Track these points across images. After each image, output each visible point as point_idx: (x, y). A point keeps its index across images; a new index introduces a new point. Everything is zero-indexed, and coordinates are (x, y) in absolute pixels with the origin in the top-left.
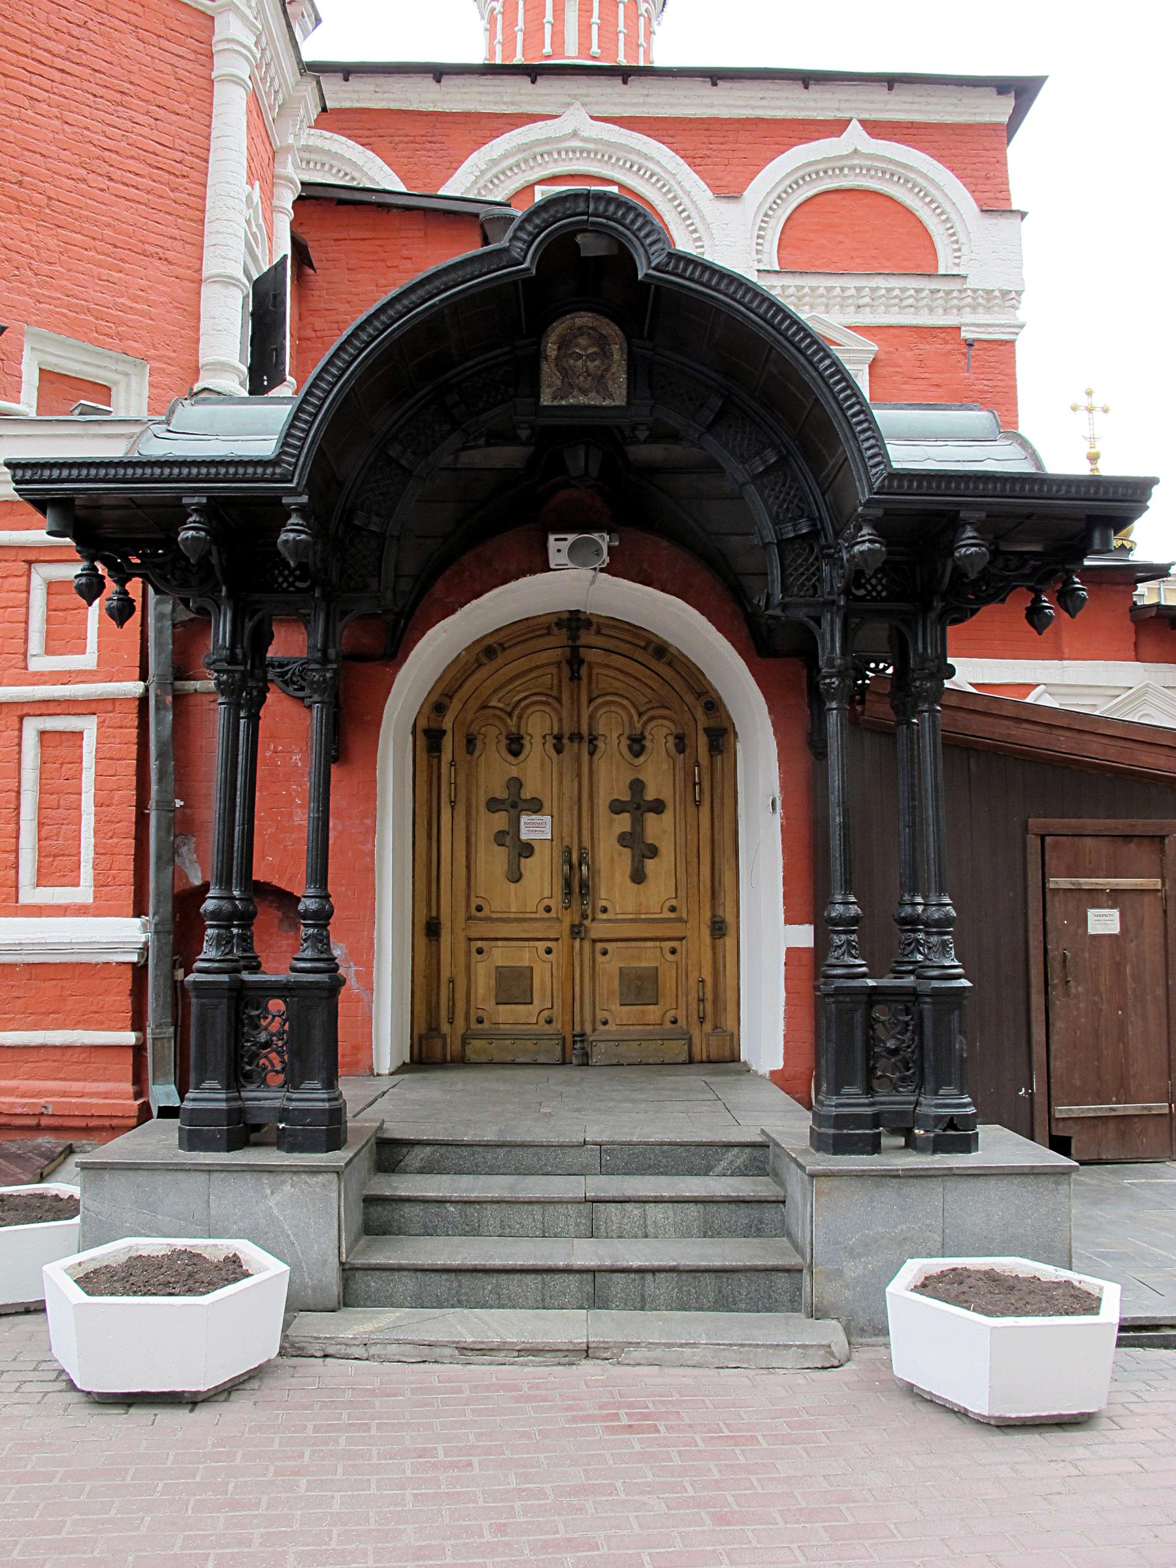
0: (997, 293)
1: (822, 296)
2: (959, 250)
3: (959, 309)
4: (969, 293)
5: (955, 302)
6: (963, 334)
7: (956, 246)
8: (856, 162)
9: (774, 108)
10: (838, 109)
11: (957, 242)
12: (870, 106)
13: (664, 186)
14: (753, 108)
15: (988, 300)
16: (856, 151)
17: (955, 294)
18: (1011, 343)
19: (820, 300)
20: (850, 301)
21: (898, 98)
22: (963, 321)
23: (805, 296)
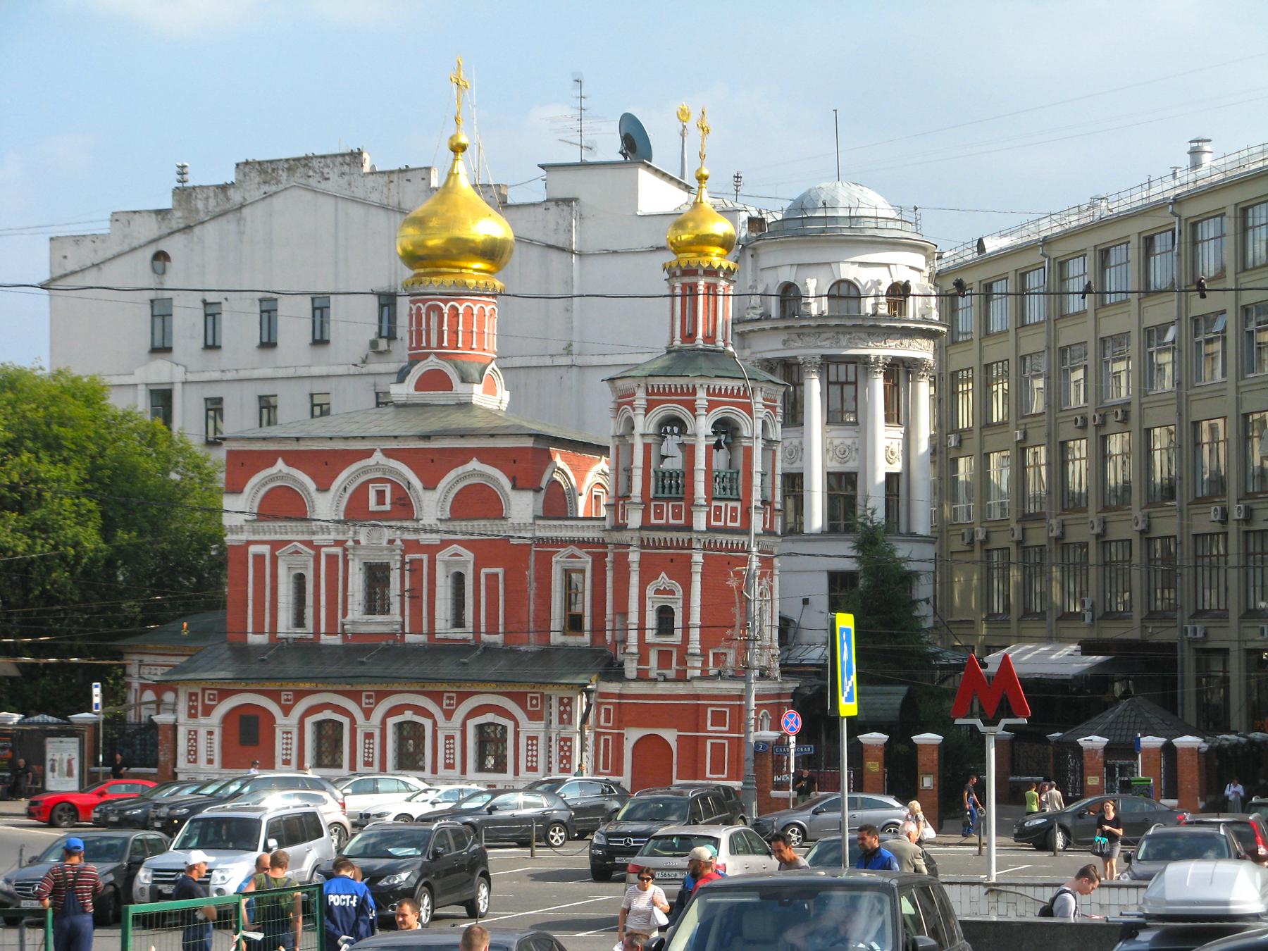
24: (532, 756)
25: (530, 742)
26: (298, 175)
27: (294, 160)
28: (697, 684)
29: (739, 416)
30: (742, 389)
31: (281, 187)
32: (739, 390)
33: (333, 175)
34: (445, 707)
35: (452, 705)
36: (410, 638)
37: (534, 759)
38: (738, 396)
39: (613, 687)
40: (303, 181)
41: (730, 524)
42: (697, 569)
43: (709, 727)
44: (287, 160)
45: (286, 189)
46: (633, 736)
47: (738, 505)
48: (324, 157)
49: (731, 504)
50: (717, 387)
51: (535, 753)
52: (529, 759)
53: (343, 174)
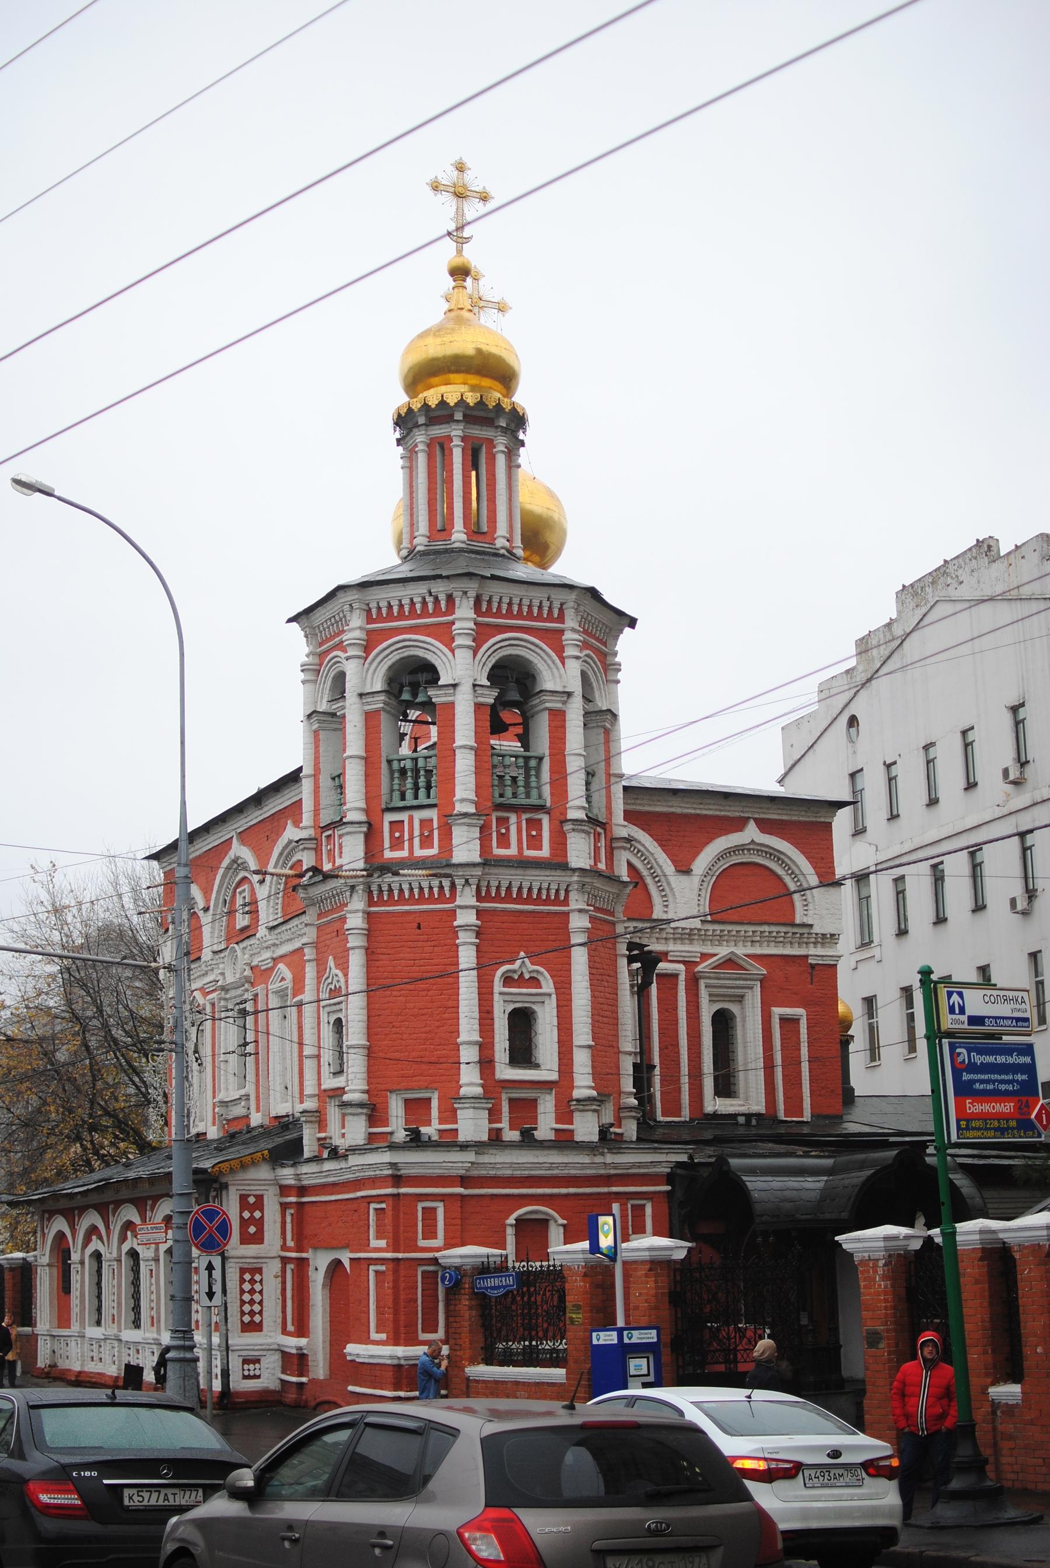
0: (828, 936)
1: (734, 936)
2: (807, 905)
3: (807, 943)
4: (814, 935)
5: (805, 940)
6: (810, 961)
7: (805, 903)
8: (751, 847)
9: (706, 809)
10: (742, 812)
11: (805, 900)
12: (760, 810)
13: (645, 859)
14: (695, 809)
15: (823, 939)
16: (753, 841)
17: (806, 935)
18: (836, 965)
19: (732, 938)
20: (749, 939)
21: (775, 807)
22: (811, 953)
23: (724, 935)
26: (940, 587)
27: (936, 570)
28: (354, 1160)
29: (434, 652)
30: (430, 600)
31: (929, 606)
32: (424, 603)
33: (963, 575)
36: (256, 1119)
38: (425, 613)
39: (287, 1174)
40: (943, 593)
41: (419, 852)
42: (355, 941)
43: (374, 1243)
44: (930, 573)
45: (932, 607)
46: (320, 1262)
47: (433, 814)
48: (957, 557)
49: (418, 815)
50: (383, 604)
53: (973, 571)
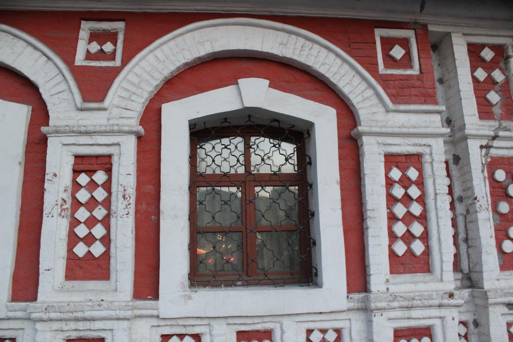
24: (409, 218)
25: (396, 174)
34: (80, 59)
35: (112, 56)
37: (417, 229)
51: (416, 209)
52: (400, 229)
